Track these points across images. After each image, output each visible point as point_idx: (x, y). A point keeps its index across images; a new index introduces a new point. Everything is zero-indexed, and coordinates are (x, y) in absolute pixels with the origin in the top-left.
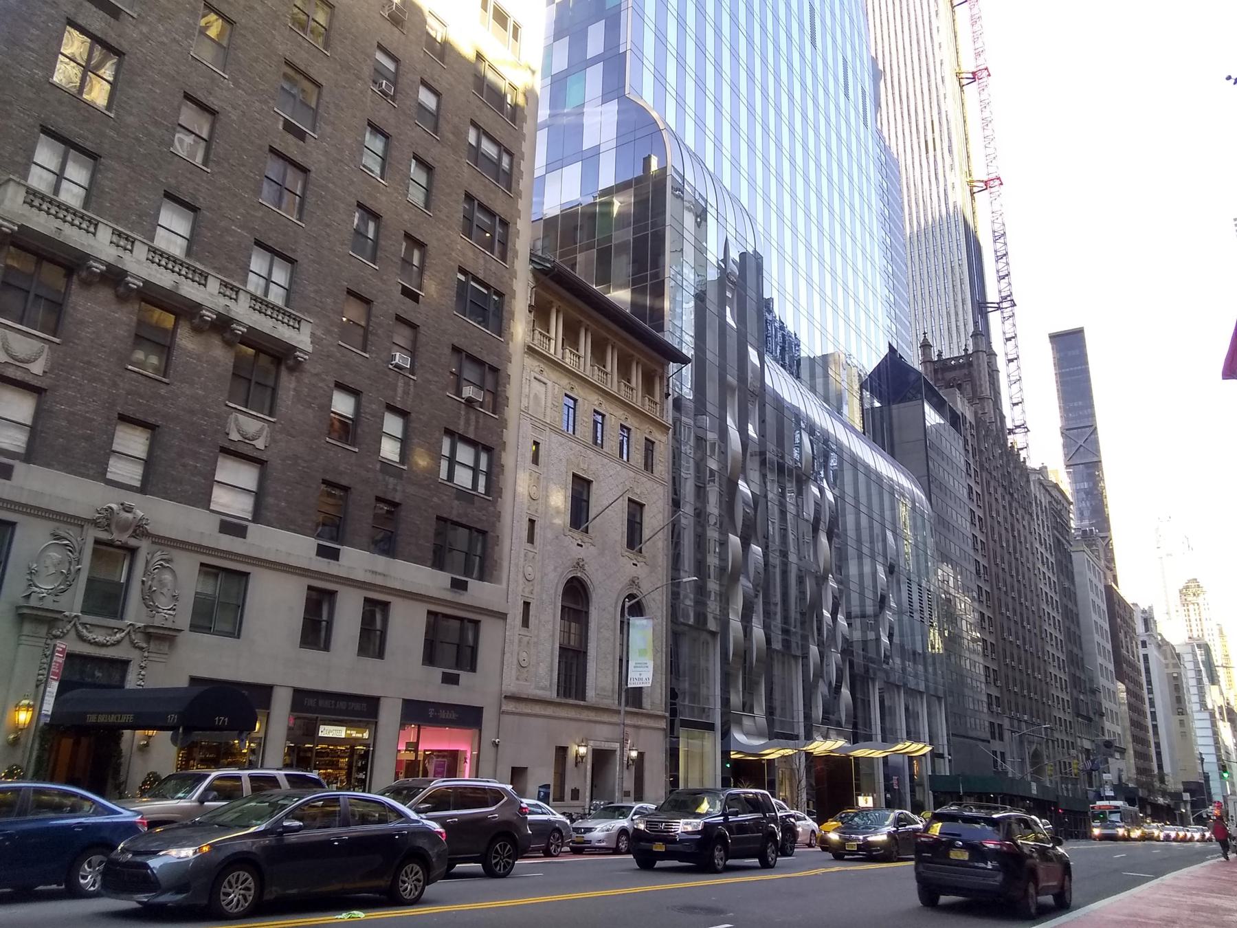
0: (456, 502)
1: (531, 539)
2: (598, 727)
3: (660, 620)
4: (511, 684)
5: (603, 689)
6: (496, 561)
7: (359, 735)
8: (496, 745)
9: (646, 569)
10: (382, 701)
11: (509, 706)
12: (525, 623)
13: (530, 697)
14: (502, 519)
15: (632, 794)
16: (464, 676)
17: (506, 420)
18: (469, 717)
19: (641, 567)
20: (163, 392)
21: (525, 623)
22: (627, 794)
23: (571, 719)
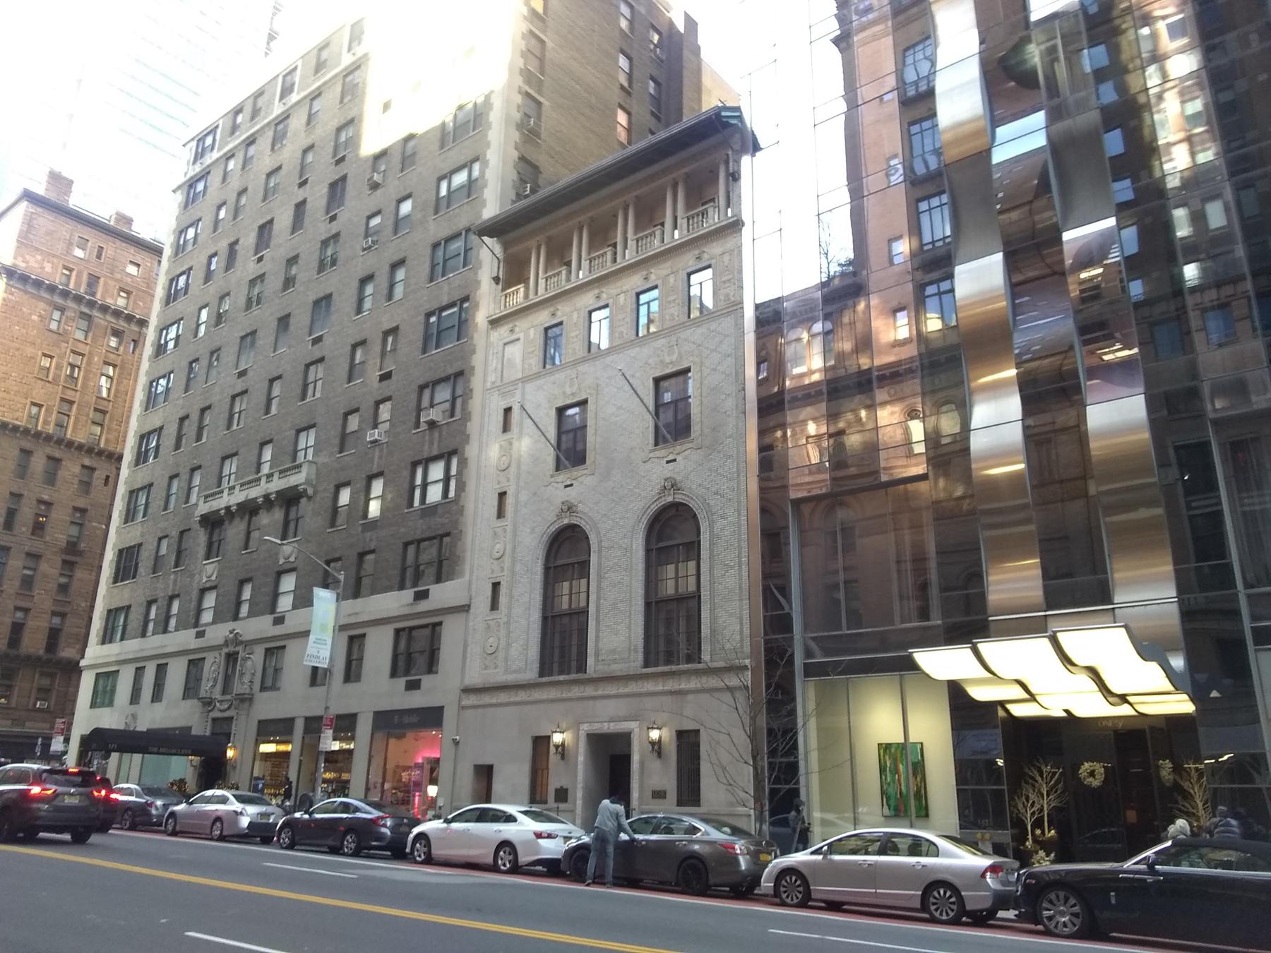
0: (421, 521)
1: (500, 514)
2: (599, 704)
3: (733, 519)
4: (475, 677)
5: (613, 651)
6: (459, 556)
7: (348, 747)
8: (456, 743)
9: (696, 456)
10: (359, 716)
11: (471, 700)
12: (494, 605)
13: (487, 686)
14: (465, 513)
15: (672, 795)
16: (427, 680)
17: (470, 413)
18: (432, 717)
19: (685, 458)
20: (255, 557)
21: (494, 605)
22: (659, 795)
23: (553, 701)
